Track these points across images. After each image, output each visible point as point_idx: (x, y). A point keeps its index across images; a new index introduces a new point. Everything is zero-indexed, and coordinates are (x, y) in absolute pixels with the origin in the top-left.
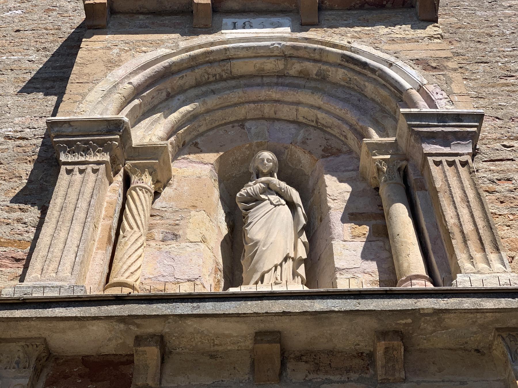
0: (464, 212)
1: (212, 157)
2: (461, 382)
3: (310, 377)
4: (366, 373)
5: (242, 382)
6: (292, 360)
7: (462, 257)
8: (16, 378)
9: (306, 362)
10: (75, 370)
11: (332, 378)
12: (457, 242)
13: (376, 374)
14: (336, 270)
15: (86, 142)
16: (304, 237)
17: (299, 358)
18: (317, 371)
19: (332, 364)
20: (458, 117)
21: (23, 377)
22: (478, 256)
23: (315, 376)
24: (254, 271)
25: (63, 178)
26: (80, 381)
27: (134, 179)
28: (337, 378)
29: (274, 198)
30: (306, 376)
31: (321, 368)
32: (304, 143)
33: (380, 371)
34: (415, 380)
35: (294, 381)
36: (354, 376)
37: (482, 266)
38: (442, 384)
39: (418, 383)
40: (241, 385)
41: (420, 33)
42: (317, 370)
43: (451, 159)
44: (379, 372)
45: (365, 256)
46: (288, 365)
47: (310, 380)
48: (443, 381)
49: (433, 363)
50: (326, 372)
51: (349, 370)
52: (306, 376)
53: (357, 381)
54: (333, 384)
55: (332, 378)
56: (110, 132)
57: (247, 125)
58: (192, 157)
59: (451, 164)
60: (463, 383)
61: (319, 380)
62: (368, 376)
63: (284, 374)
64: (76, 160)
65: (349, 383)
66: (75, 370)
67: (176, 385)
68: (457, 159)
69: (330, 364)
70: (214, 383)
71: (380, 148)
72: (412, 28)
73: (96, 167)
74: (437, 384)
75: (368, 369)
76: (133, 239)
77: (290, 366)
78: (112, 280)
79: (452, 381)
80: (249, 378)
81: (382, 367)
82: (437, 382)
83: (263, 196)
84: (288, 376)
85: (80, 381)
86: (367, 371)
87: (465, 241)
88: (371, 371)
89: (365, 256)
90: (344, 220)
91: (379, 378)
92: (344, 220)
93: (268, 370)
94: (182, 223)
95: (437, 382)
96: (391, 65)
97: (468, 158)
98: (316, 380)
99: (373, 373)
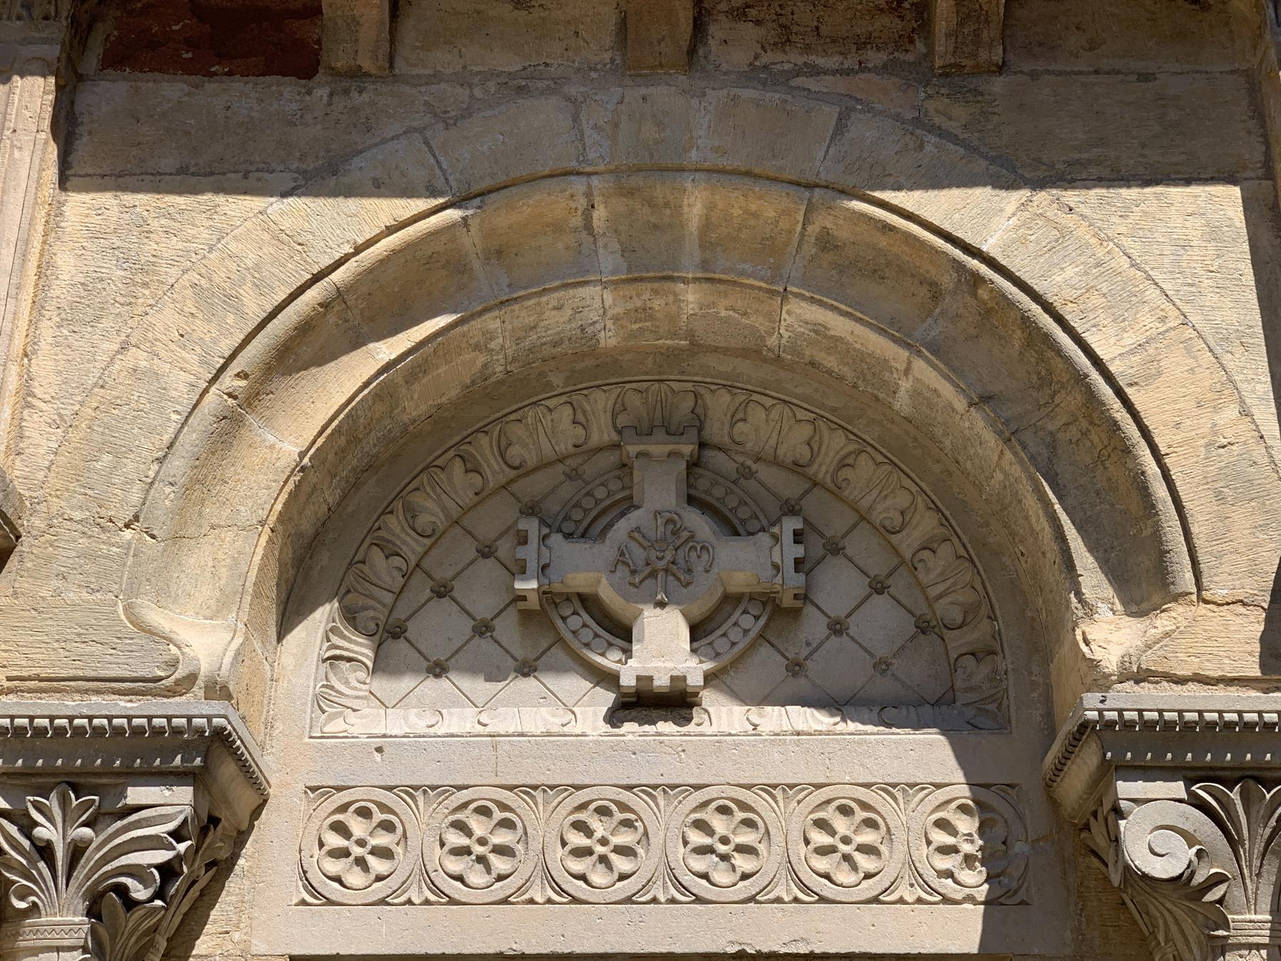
2: (1139, 74)
3: (765, 59)
4: (907, 51)
5: (595, 70)
6: (722, 17)
8: (26, 42)
9: (758, 23)
10: (174, 28)
11: (820, 61)
13: (931, 52)
18: (783, 44)
19: (822, 28)
21: (45, 41)
23: (779, 56)
26: (190, 55)
28: (831, 62)
30: (756, 57)
31: (794, 38)
33: (942, 46)
34: (1027, 67)
35: (724, 67)
36: (875, 57)
38: (1092, 78)
39: (1034, 75)
40: (593, 75)
42: (785, 40)
44: (939, 48)
46: (712, 29)
47: (765, 67)
48: (1097, 72)
49: (1078, 28)
50: (808, 49)
51: (863, 43)
52: (756, 57)
53: (885, 69)
54: (822, 76)
55: (820, 61)
60: (1145, 77)
61: (787, 67)
62: (910, 57)
63: (701, 52)
65: (863, 76)
66: (174, 28)
67: (430, 72)
69: (817, 28)
70: (524, 69)
74: (1082, 79)
75: (911, 41)
77: (716, 31)
79: (1118, 72)
80: (612, 60)
81: (948, 36)
82: (1081, 73)
84: (712, 58)
85: (190, 55)
86: (909, 47)
88: (920, 46)
91: (938, 63)
93: (659, 42)
95: (1081, 73)
98: (778, 66)
99: (924, 50)
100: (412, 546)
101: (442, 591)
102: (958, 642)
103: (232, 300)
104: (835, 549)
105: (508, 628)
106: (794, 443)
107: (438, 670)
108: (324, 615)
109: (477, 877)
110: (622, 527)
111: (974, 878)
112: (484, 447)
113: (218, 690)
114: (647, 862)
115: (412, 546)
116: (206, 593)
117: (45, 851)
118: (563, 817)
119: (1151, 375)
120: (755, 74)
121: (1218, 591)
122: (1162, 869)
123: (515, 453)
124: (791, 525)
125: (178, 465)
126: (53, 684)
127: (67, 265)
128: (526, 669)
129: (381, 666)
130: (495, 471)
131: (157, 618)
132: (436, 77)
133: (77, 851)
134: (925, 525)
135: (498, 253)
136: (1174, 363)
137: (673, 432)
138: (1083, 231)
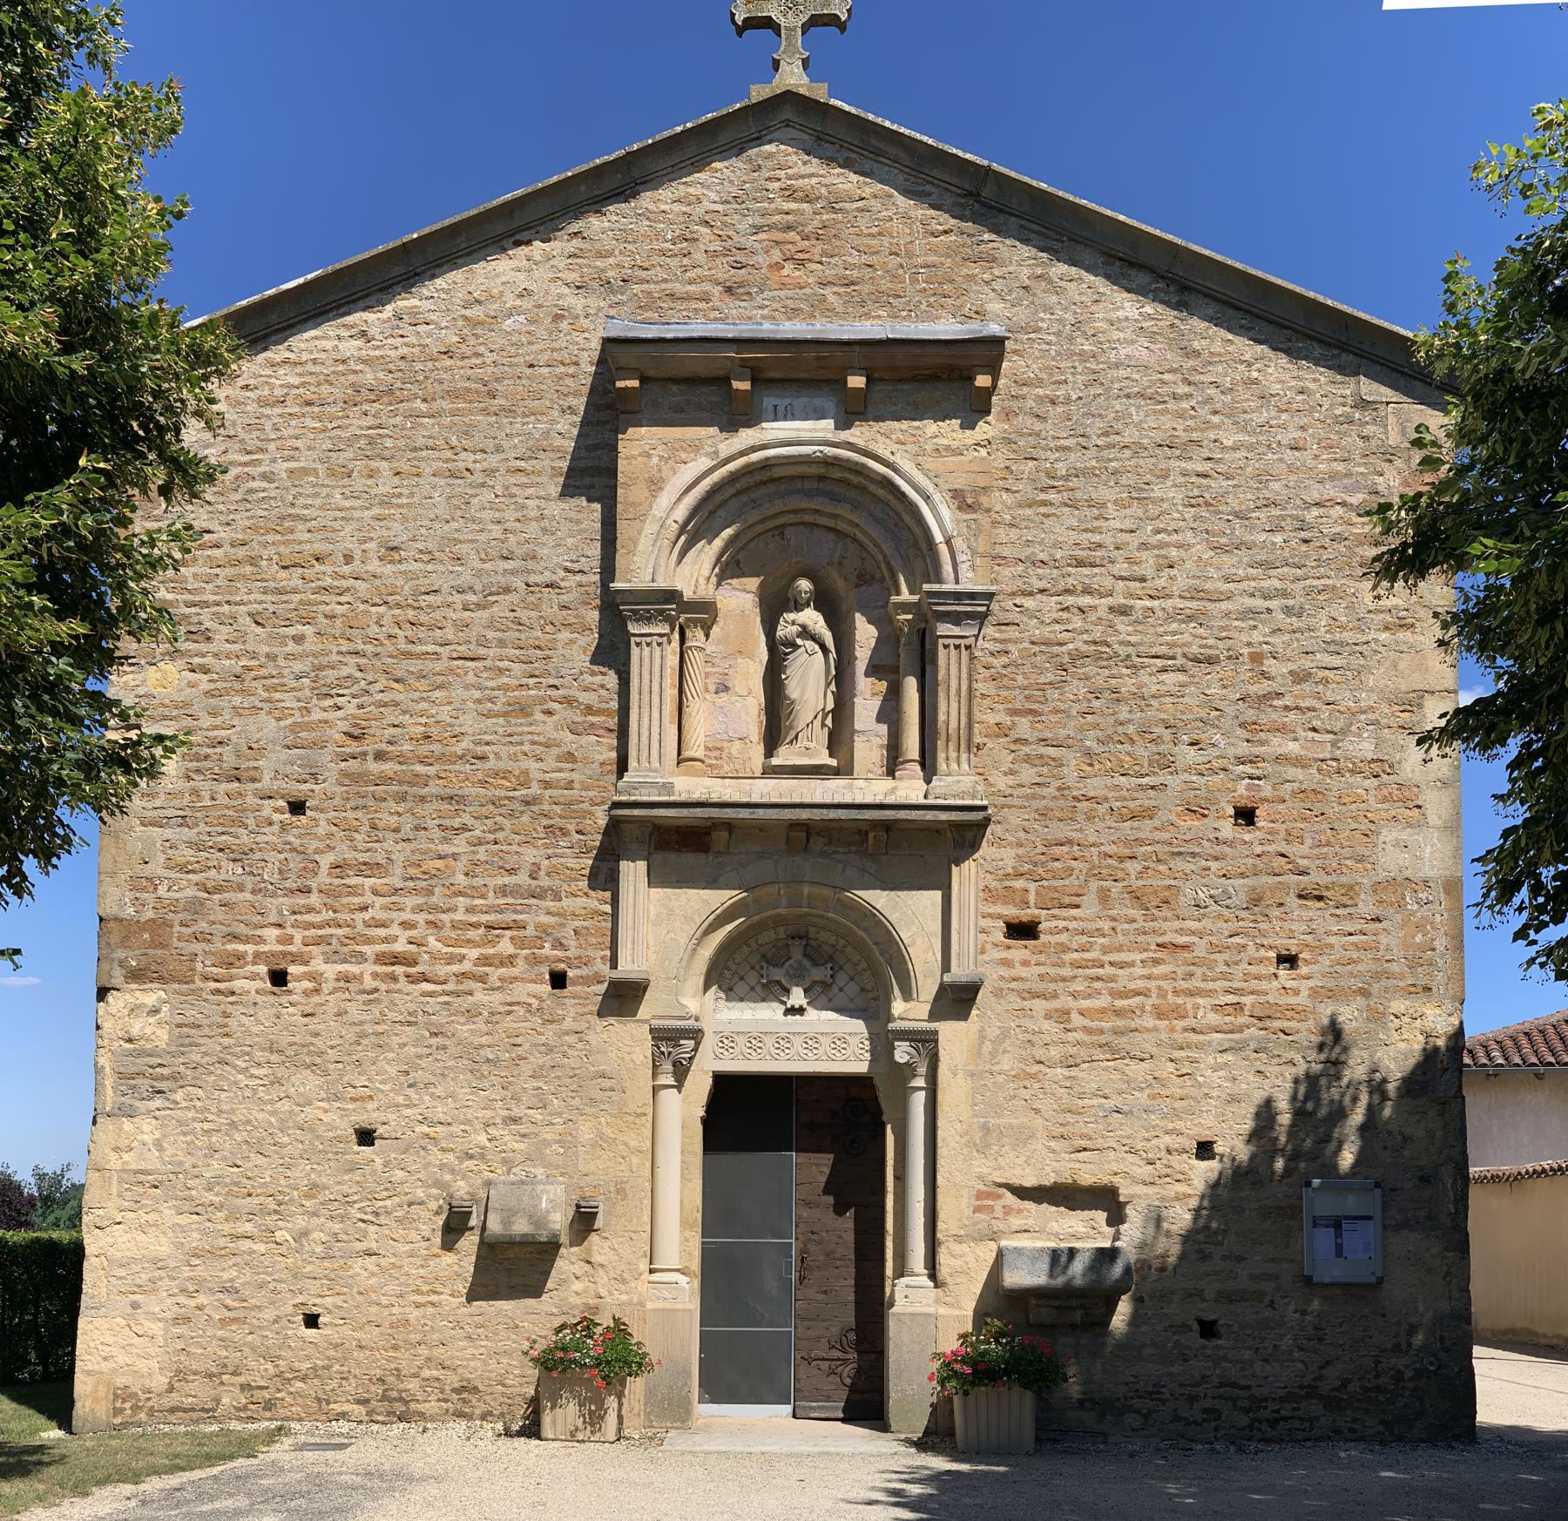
0: (954, 705)
1: (753, 583)
7: (941, 756)
12: (940, 744)
14: (854, 731)
15: (648, 611)
16: (833, 687)
17: (818, 834)
20: (972, 596)
22: (953, 755)
24: (791, 727)
25: (635, 651)
27: (689, 634)
29: (810, 644)
32: (840, 563)
36: (854, 849)
37: (954, 766)
41: (970, 436)
42: (830, 844)
43: (957, 642)
45: (879, 719)
53: (855, 853)
56: (667, 602)
57: (788, 532)
58: (734, 582)
59: (957, 647)
60: (922, 856)
64: (644, 631)
68: (963, 642)
71: (905, 607)
72: (962, 427)
73: (660, 640)
76: (696, 710)
77: (812, 839)
78: (686, 754)
83: (799, 641)
87: (948, 741)
89: (879, 719)
90: (867, 674)
92: (867, 674)
94: (731, 671)
96: (927, 498)
97: (971, 641)
100: (734, 967)
101: (742, 978)
102: (871, 995)
103: (692, 919)
104: (841, 968)
105: (758, 988)
106: (832, 940)
107: (742, 1000)
108: (714, 988)
109: (754, 1054)
110: (787, 964)
111: (868, 1055)
112: (752, 942)
113: (697, 1019)
114: (793, 1051)
115: (734, 967)
116: (691, 992)
117: (663, 1053)
118: (774, 1040)
119: (914, 943)
120: (823, 854)
121: (921, 999)
122: (902, 1061)
123: (760, 942)
124: (830, 965)
125: (684, 964)
126: (662, 1017)
127: (653, 911)
128: (764, 1000)
129: (728, 1000)
130: (754, 946)
131: (684, 1001)
132: (740, 853)
133: (670, 1053)
134: (864, 965)
135: (756, 901)
136: (919, 941)
137: (801, 938)
138: (901, 903)
